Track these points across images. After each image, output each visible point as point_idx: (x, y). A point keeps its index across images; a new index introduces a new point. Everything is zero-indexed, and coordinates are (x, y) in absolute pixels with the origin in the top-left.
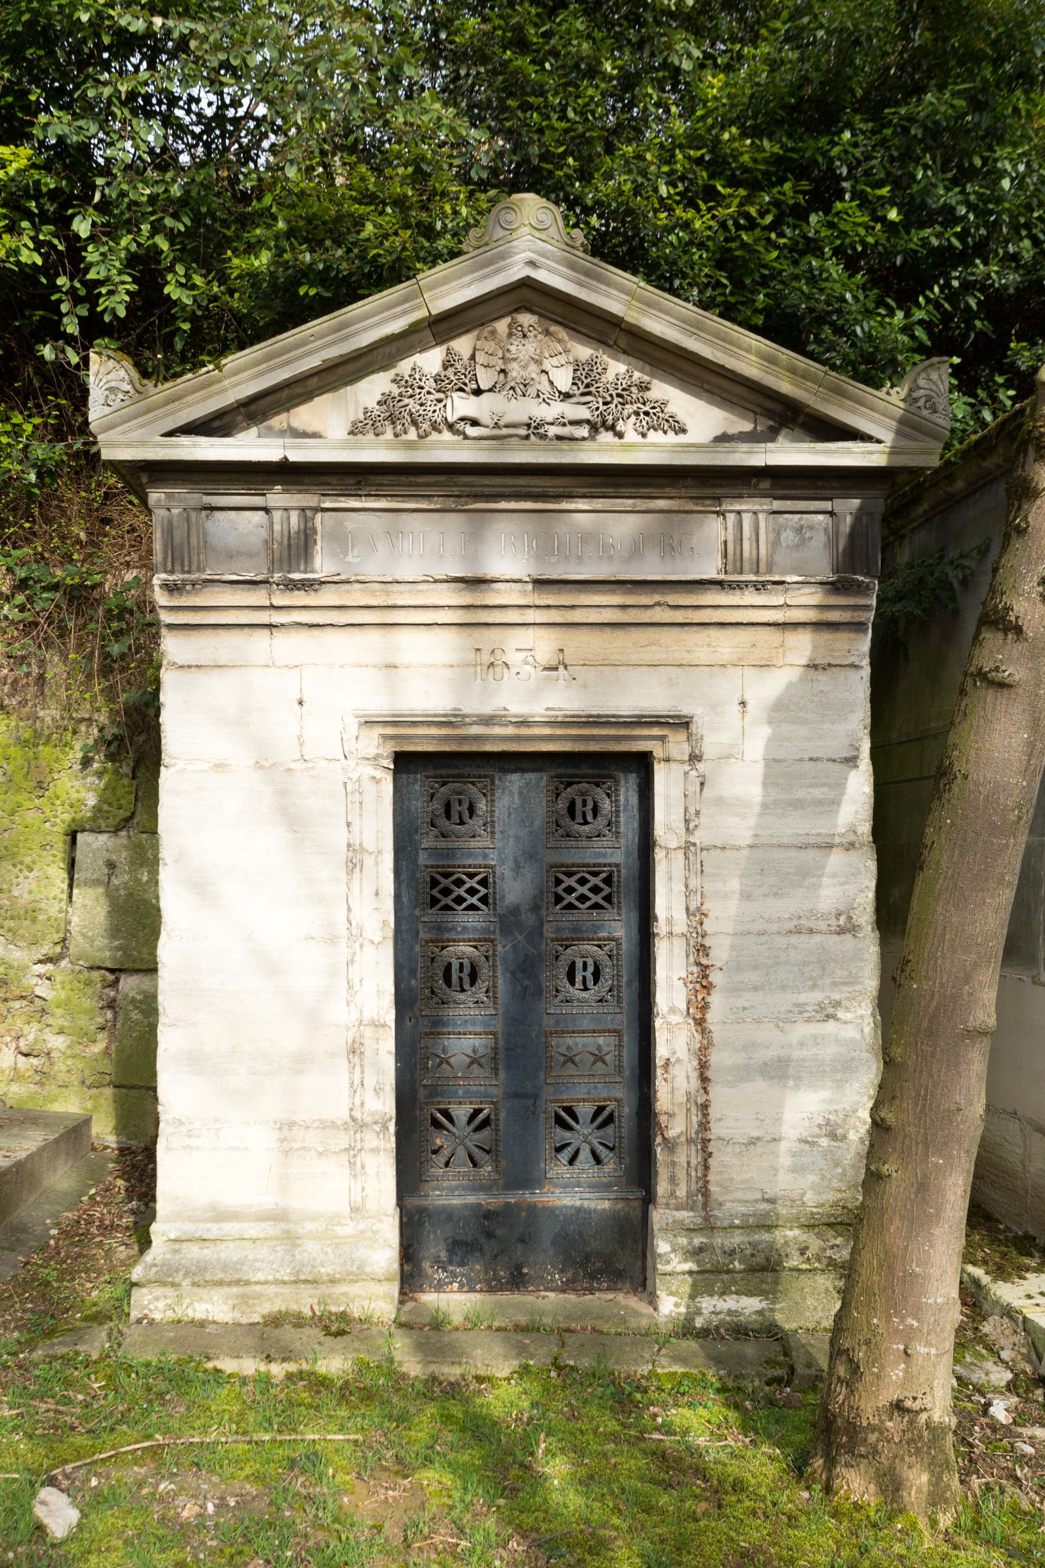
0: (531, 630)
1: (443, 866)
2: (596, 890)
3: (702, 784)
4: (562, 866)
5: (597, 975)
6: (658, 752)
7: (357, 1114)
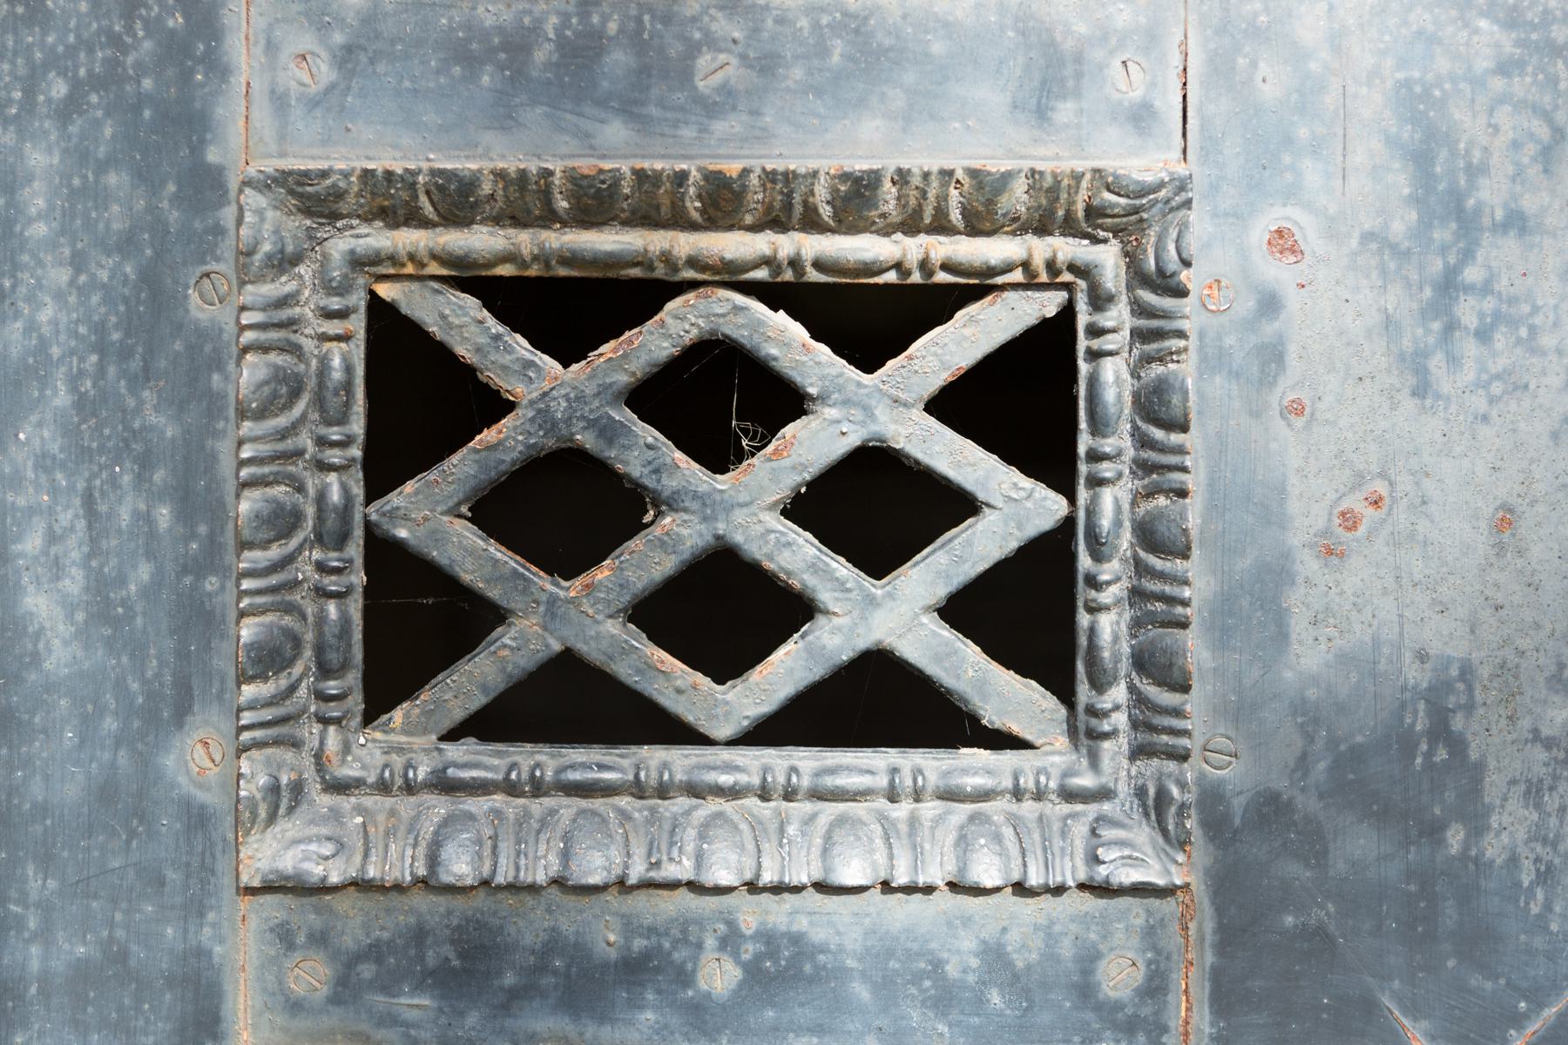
1: (525, 201)
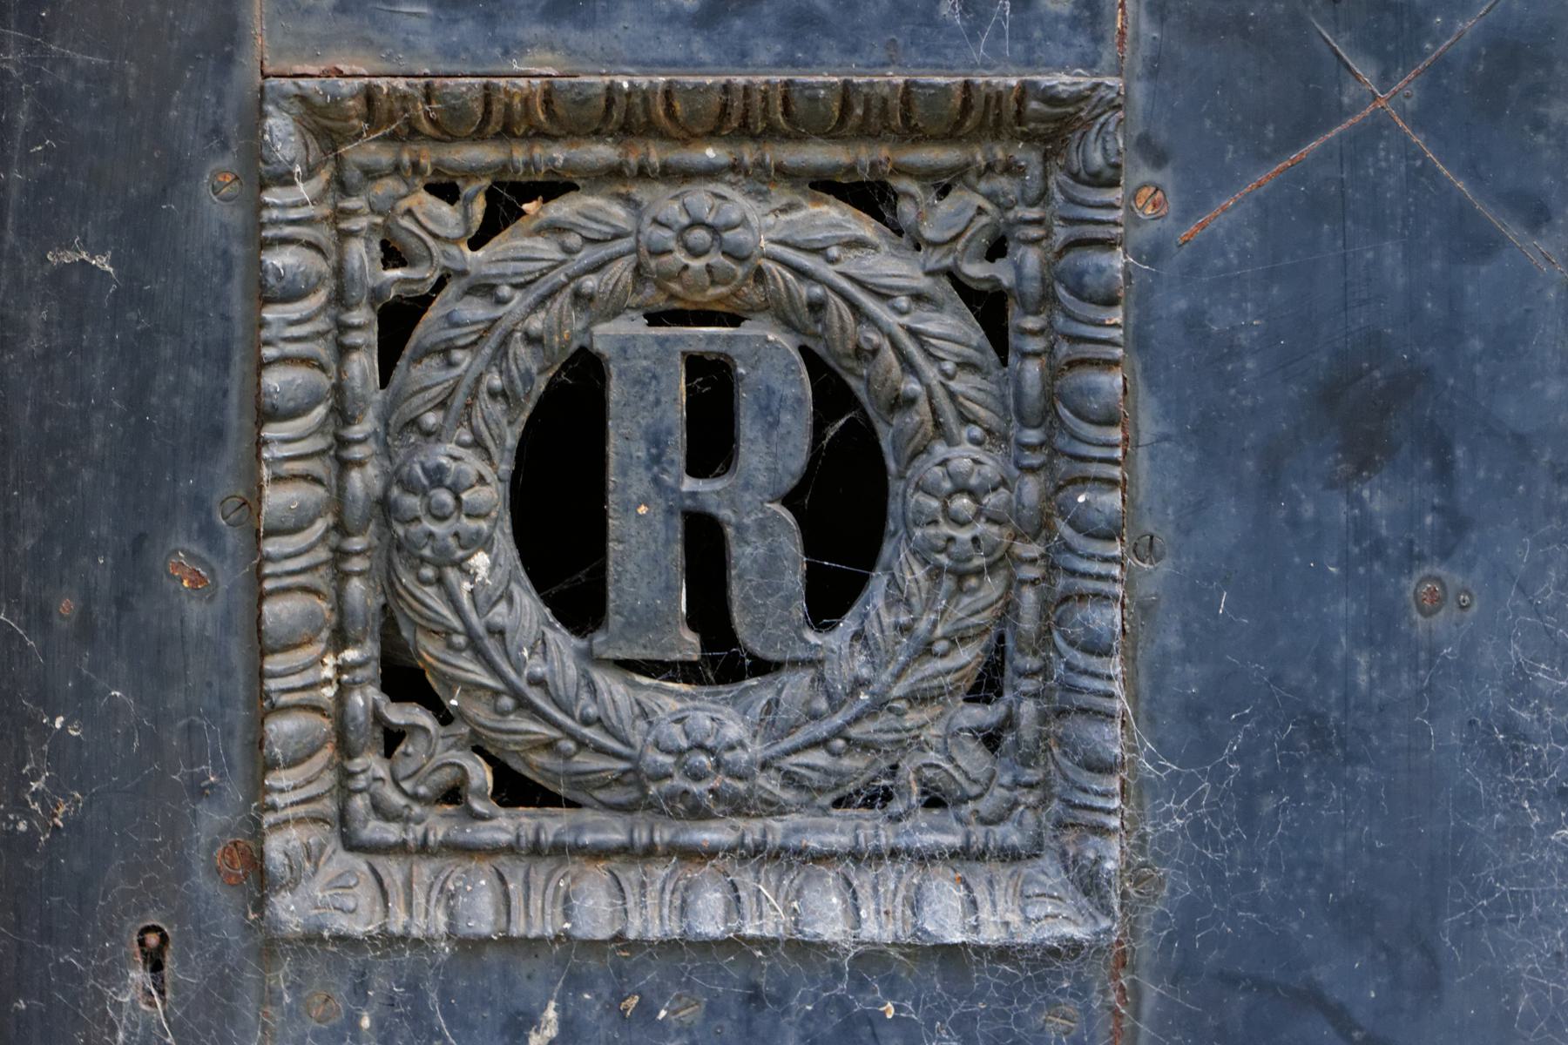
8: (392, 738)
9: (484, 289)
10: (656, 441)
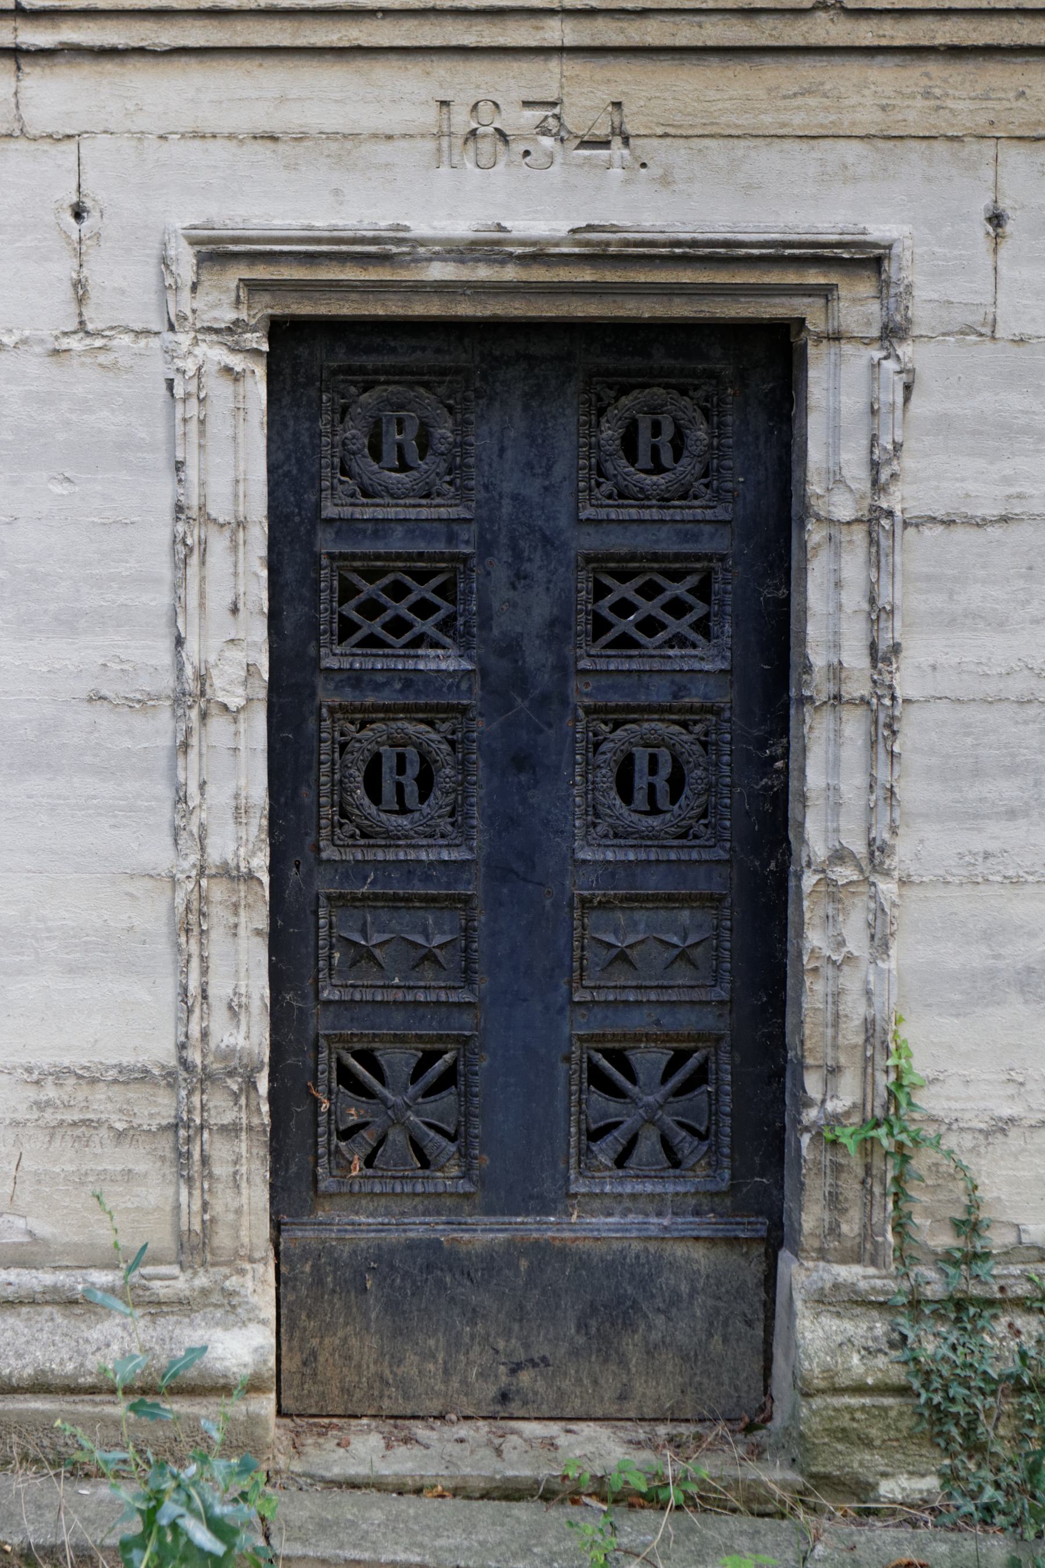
0: (554, 64)
2: (677, 608)
3: (908, 388)
4: (610, 557)
5: (677, 783)
6: (815, 317)
7: (195, 1056)
8: (341, 825)
9: (359, 741)
10: (391, 768)
